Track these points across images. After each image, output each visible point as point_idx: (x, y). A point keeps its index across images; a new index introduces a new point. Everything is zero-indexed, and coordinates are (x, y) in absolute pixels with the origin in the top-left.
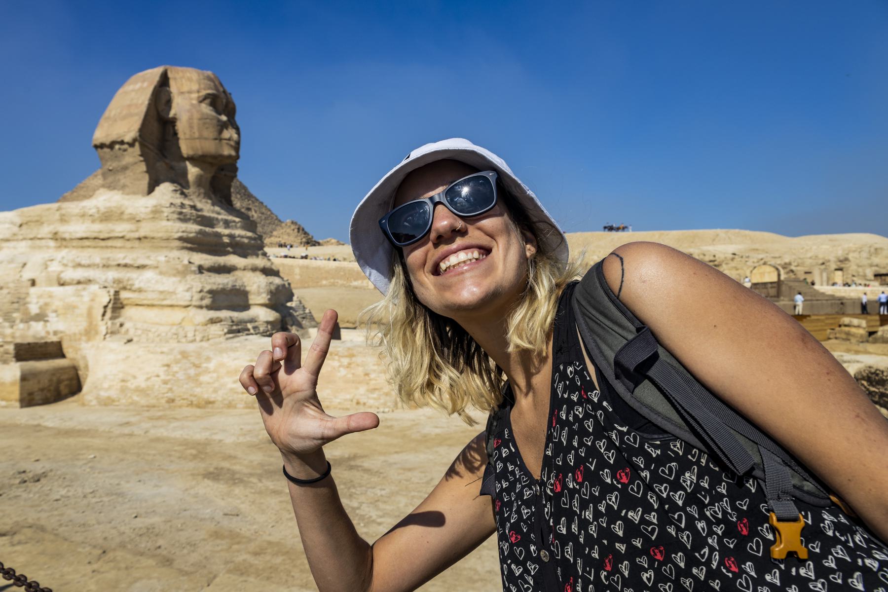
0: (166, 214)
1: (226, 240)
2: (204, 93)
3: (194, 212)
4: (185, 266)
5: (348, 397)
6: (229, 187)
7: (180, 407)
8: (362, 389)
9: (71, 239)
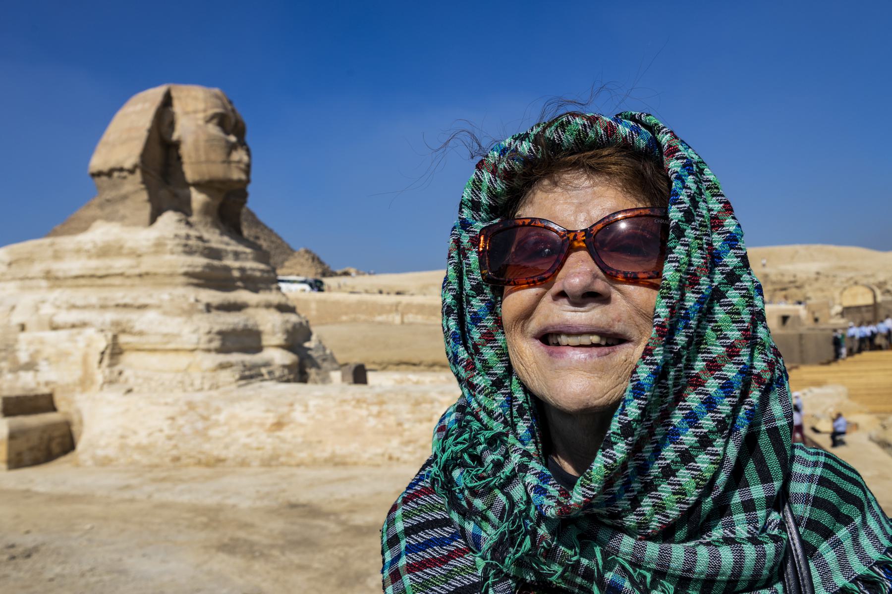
0: (169, 247)
1: (236, 274)
2: (211, 112)
3: (200, 244)
4: (192, 305)
5: (379, 451)
6: (238, 215)
7: (187, 466)
8: (395, 442)
9: (66, 278)
